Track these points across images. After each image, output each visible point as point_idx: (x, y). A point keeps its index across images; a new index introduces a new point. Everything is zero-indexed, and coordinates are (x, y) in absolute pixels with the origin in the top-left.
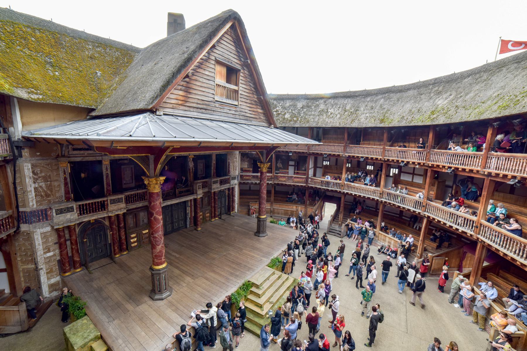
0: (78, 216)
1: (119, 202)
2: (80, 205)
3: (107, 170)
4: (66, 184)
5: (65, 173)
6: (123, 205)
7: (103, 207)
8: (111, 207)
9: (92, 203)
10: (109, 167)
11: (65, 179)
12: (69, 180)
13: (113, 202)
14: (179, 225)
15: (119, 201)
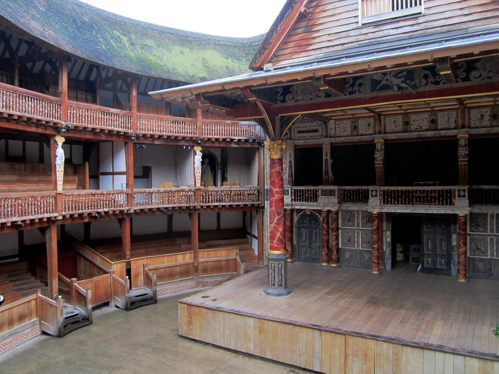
0: (292, 201)
1: (331, 195)
2: (295, 190)
3: (327, 155)
4: (290, 167)
5: (290, 157)
6: (335, 200)
7: (314, 197)
8: (322, 199)
9: (305, 190)
10: (329, 152)
11: (290, 162)
12: (293, 163)
13: (326, 193)
14: (434, 262)
15: (331, 193)
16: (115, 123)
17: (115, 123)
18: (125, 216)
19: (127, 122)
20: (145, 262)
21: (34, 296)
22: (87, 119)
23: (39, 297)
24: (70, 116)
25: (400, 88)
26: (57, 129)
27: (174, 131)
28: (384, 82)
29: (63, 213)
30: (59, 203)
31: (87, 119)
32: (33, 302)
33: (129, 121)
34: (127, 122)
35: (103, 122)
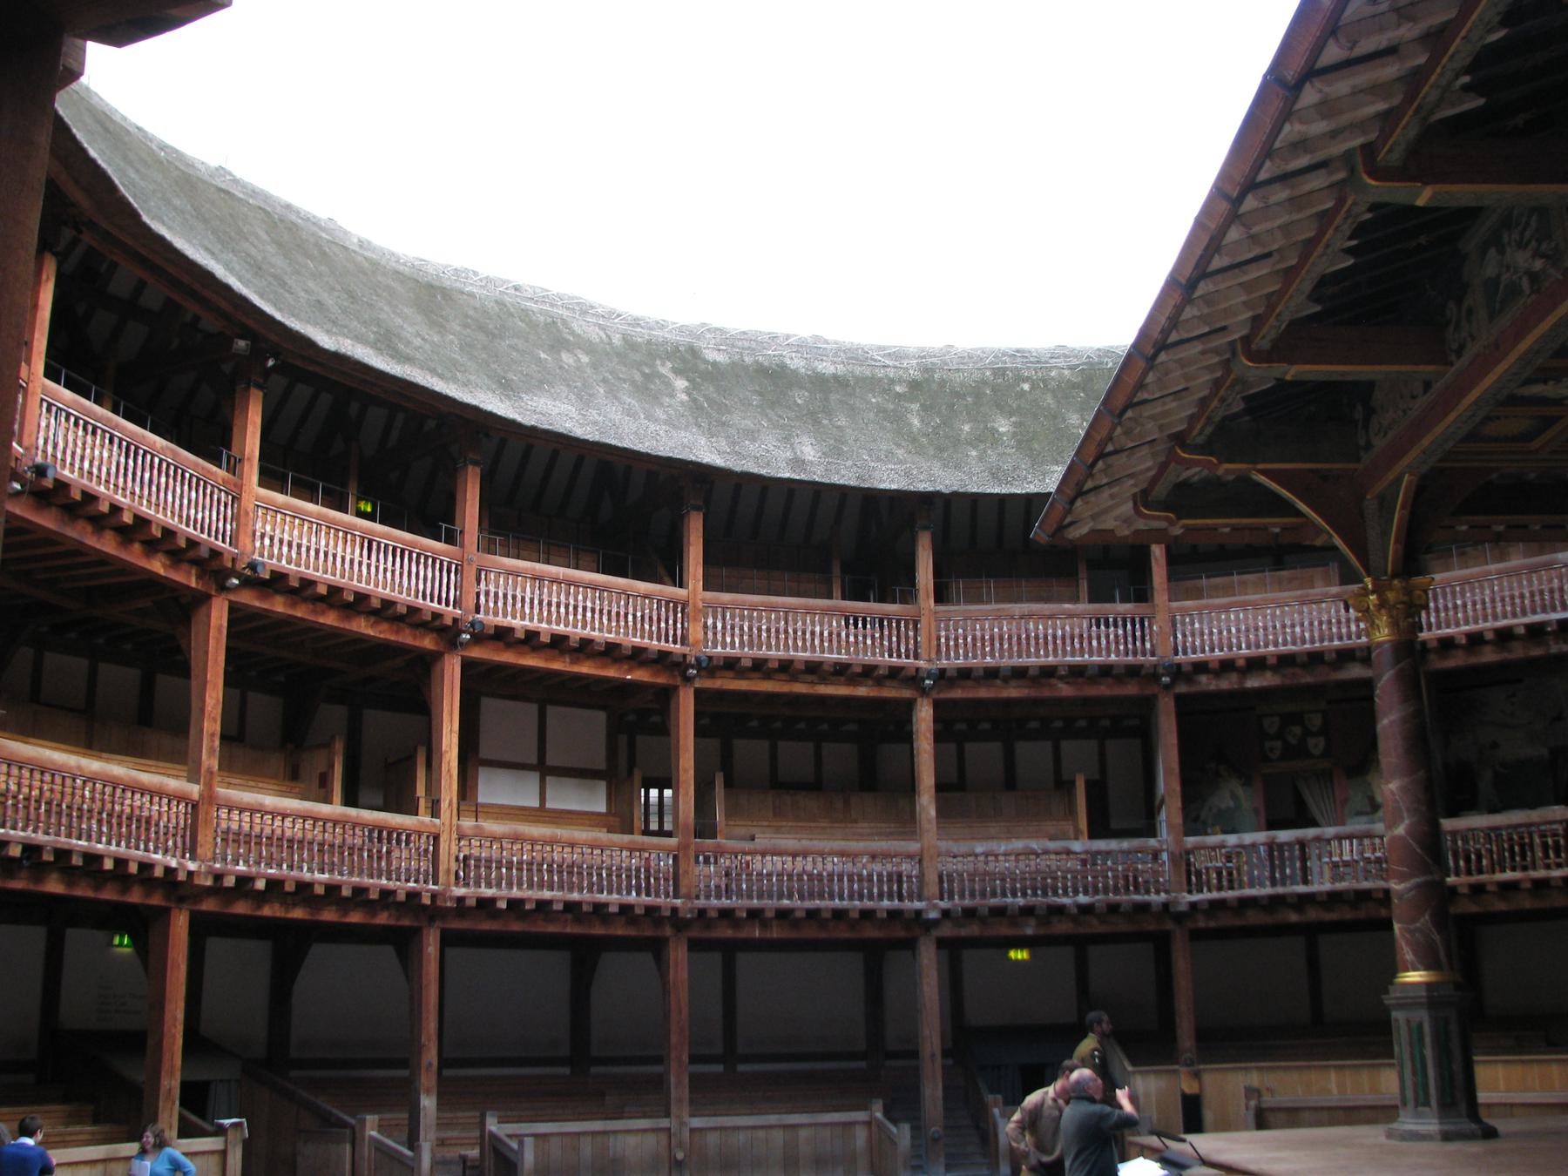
16: (1095, 643)
17: (1095, 643)
18: (1169, 925)
19: (1138, 634)
20: (1254, 1079)
21: (861, 1116)
22: (997, 645)
23: (877, 1120)
24: (948, 646)
25: (1534, 277)
26: (913, 679)
27: (1307, 635)
28: (1505, 277)
29: (944, 904)
30: (931, 877)
31: (997, 645)
32: (861, 1136)
33: (1147, 631)
34: (1138, 634)
35: (1050, 648)
